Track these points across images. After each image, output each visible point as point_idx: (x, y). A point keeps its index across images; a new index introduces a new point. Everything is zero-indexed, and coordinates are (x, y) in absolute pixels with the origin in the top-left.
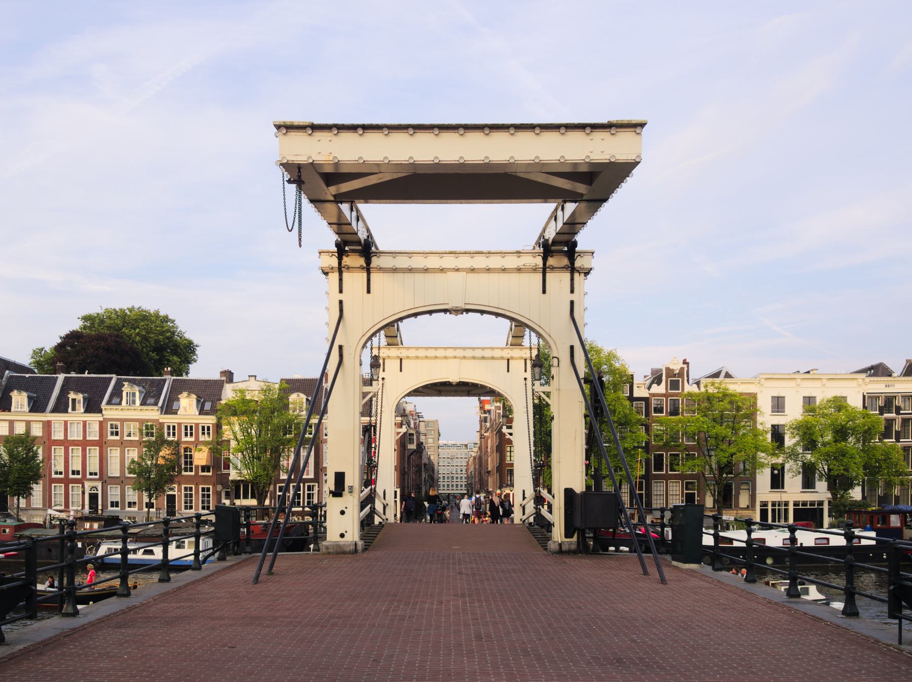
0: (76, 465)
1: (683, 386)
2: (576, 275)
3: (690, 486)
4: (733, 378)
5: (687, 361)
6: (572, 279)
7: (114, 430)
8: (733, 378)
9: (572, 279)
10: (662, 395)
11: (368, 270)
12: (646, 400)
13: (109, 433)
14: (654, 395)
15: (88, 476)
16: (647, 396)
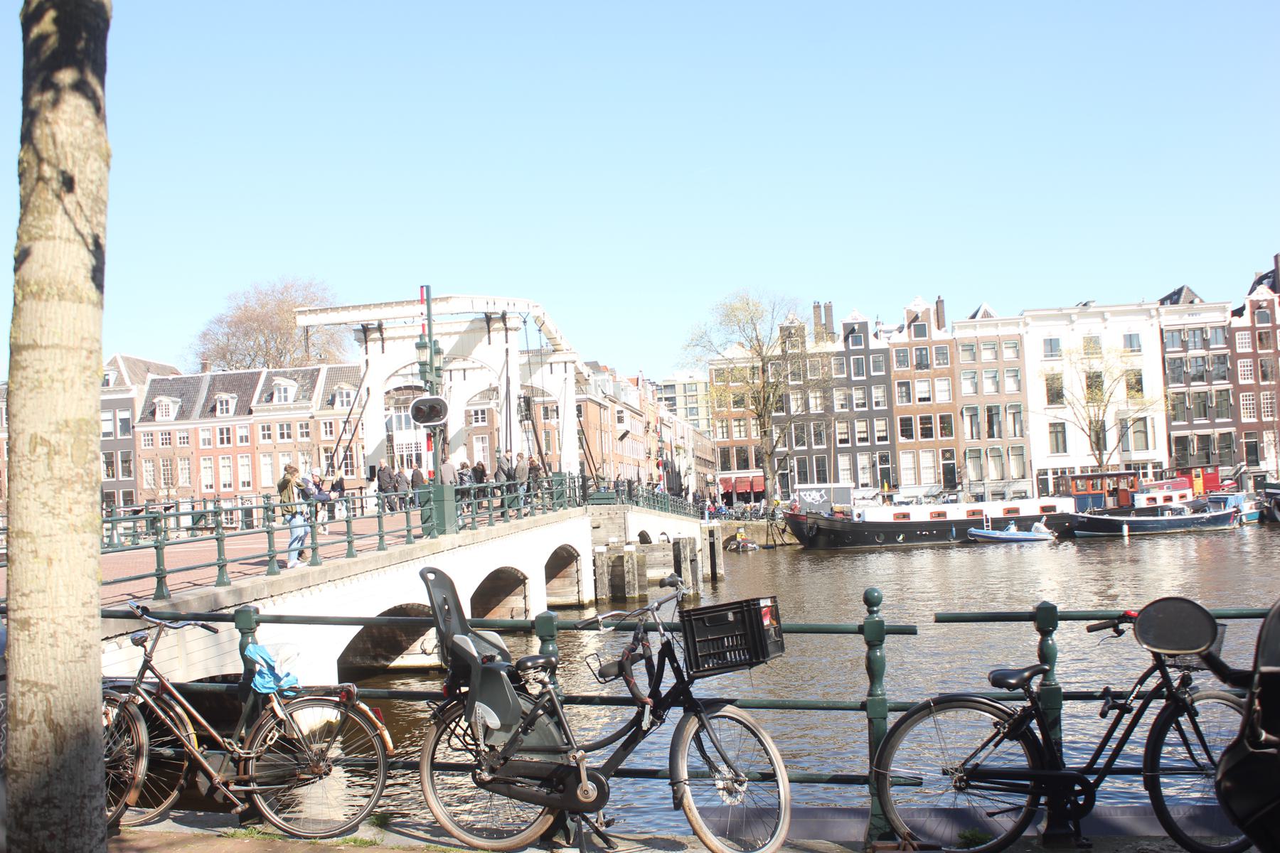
0: (225, 476)
1: (930, 331)
2: (510, 332)
3: (948, 455)
4: (991, 317)
5: (942, 299)
6: (506, 335)
7: (266, 432)
8: (991, 317)
9: (506, 335)
10: (905, 344)
11: (383, 340)
12: (885, 352)
13: (261, 437)
14: (894, 345)
15: (241, 489)
16: (887, 346)
